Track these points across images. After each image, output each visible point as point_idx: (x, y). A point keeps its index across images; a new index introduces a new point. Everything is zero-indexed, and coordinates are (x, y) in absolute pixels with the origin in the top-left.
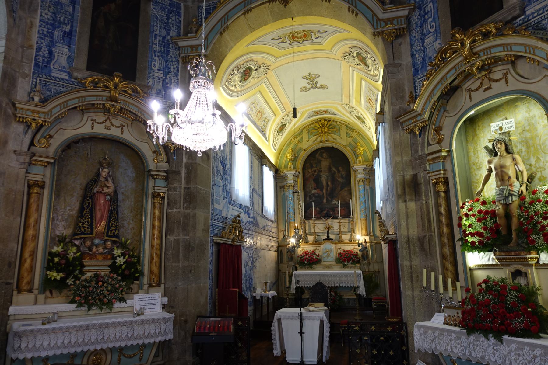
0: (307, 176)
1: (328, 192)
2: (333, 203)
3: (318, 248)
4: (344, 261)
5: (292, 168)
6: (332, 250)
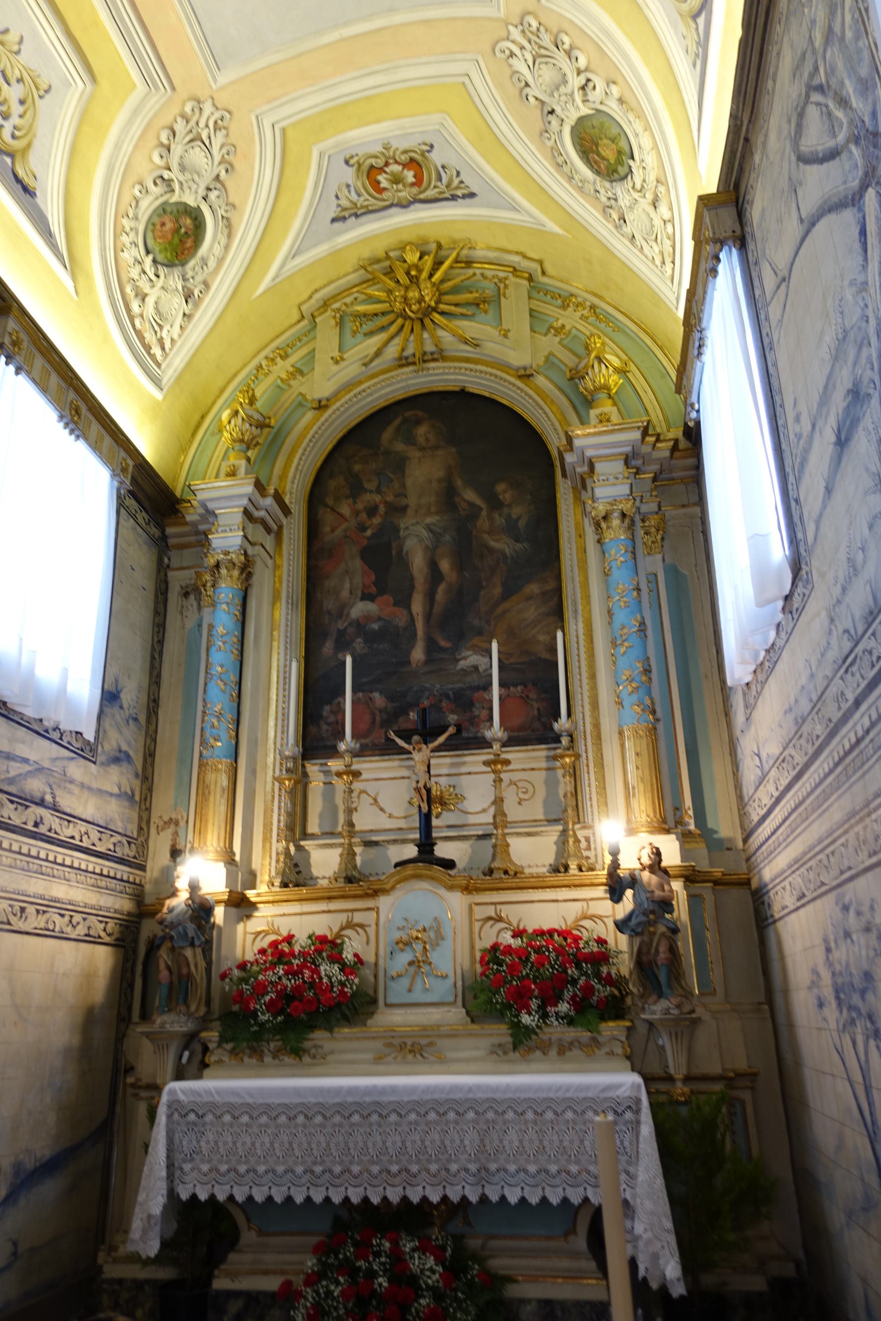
0: (331, 533)
1: (437, 609)
2: (462, 664)
3: (358, 918)
4: (520, 999)
5: (242, 471)
6: (448, 932)
